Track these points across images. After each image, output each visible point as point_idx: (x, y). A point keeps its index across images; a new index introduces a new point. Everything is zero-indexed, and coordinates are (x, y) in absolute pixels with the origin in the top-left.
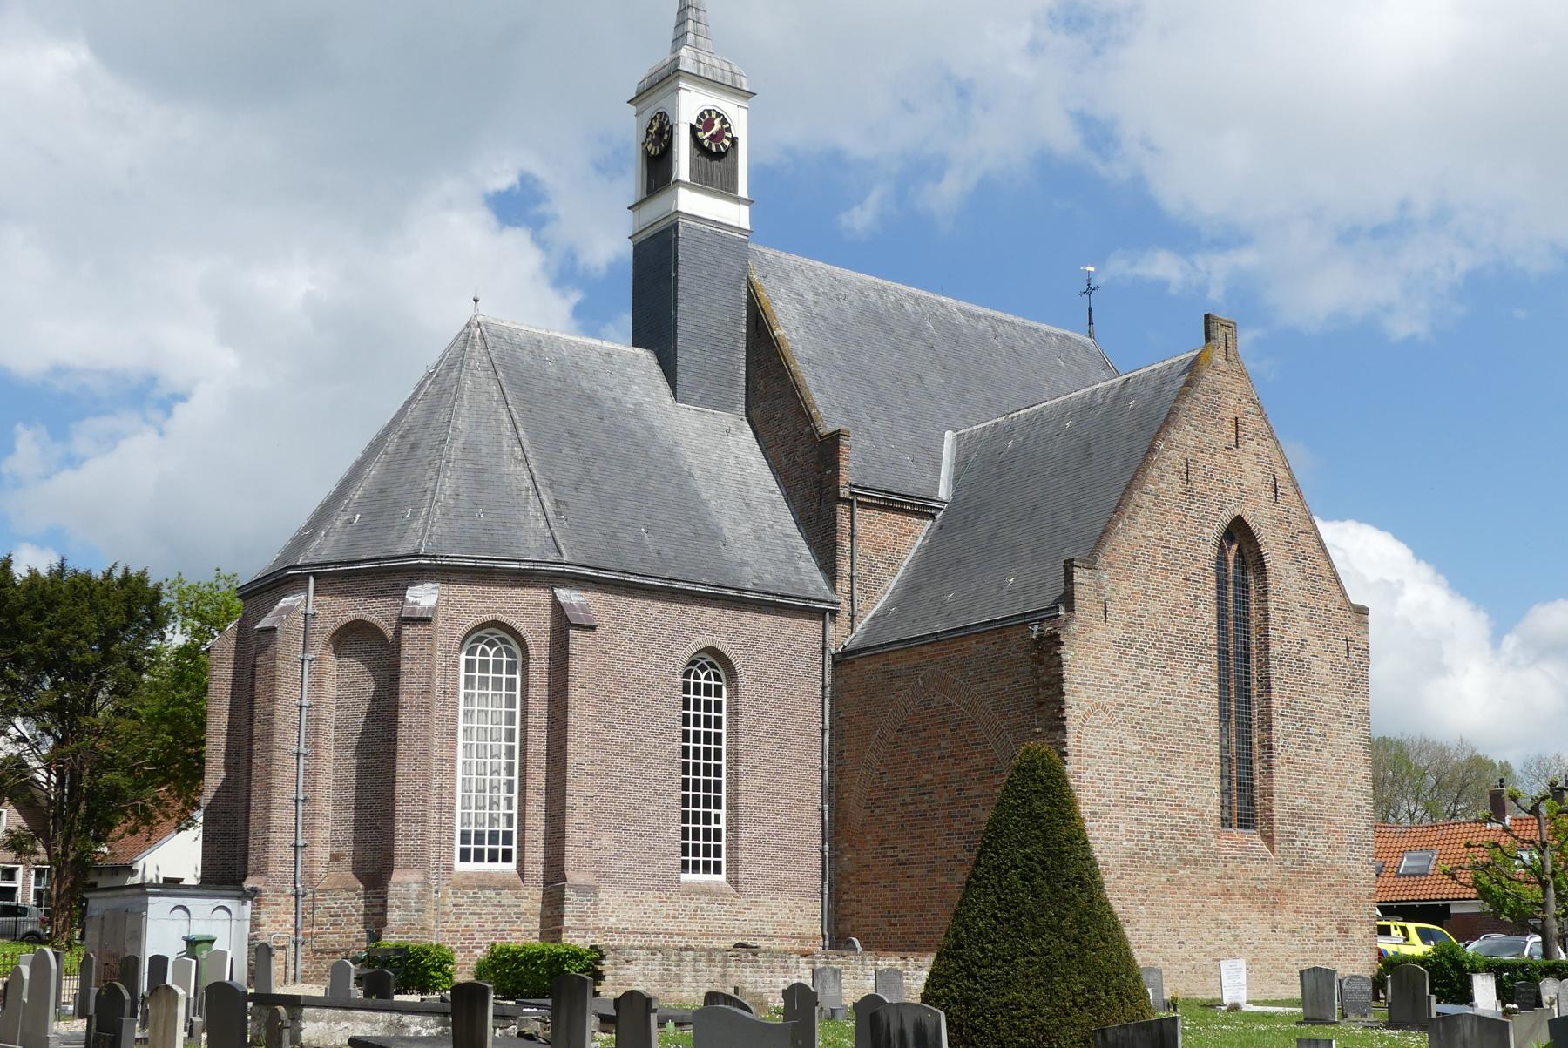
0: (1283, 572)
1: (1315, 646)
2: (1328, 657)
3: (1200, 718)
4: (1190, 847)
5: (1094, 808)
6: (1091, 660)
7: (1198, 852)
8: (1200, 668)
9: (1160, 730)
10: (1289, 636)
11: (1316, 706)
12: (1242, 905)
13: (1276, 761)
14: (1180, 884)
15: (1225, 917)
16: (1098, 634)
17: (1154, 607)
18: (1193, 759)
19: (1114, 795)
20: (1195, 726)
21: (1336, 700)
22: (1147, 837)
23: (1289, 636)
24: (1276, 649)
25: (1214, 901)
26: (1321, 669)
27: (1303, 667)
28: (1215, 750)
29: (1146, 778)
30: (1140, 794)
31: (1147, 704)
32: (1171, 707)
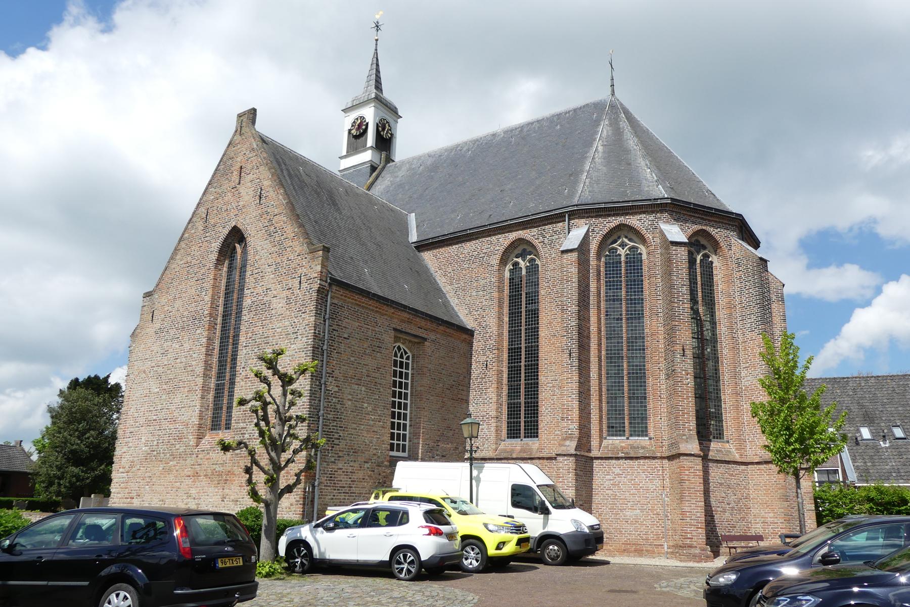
0: (258, 248)
1: (276, 289)
2: (286, 293)
3: (194, 363)
4: (177, 446)
5: (132, 430)
6: (143, 346)
7: (182, 449)
8: (198, 332)
9: (171, 376)
10: (259, 290)
11: (270, 333)
12: (204, 482)
13: (237, 379)
14: (170, 470)
15: (193, 491)
16: (148, 330)
17: (178, 304)
18: (186, 390)
19: (142, 420)
20: (190, 369)
21: (287, 323)
22: (155, 443)
23: (259, 290)
24: (247, 302)
25: (189, 481)
26: (278, 305)
27: (263, 307)
28: (200, 381)
29: (159, 407)
30: (155, 417)
31: (166, 363)
32: (178, 361)
